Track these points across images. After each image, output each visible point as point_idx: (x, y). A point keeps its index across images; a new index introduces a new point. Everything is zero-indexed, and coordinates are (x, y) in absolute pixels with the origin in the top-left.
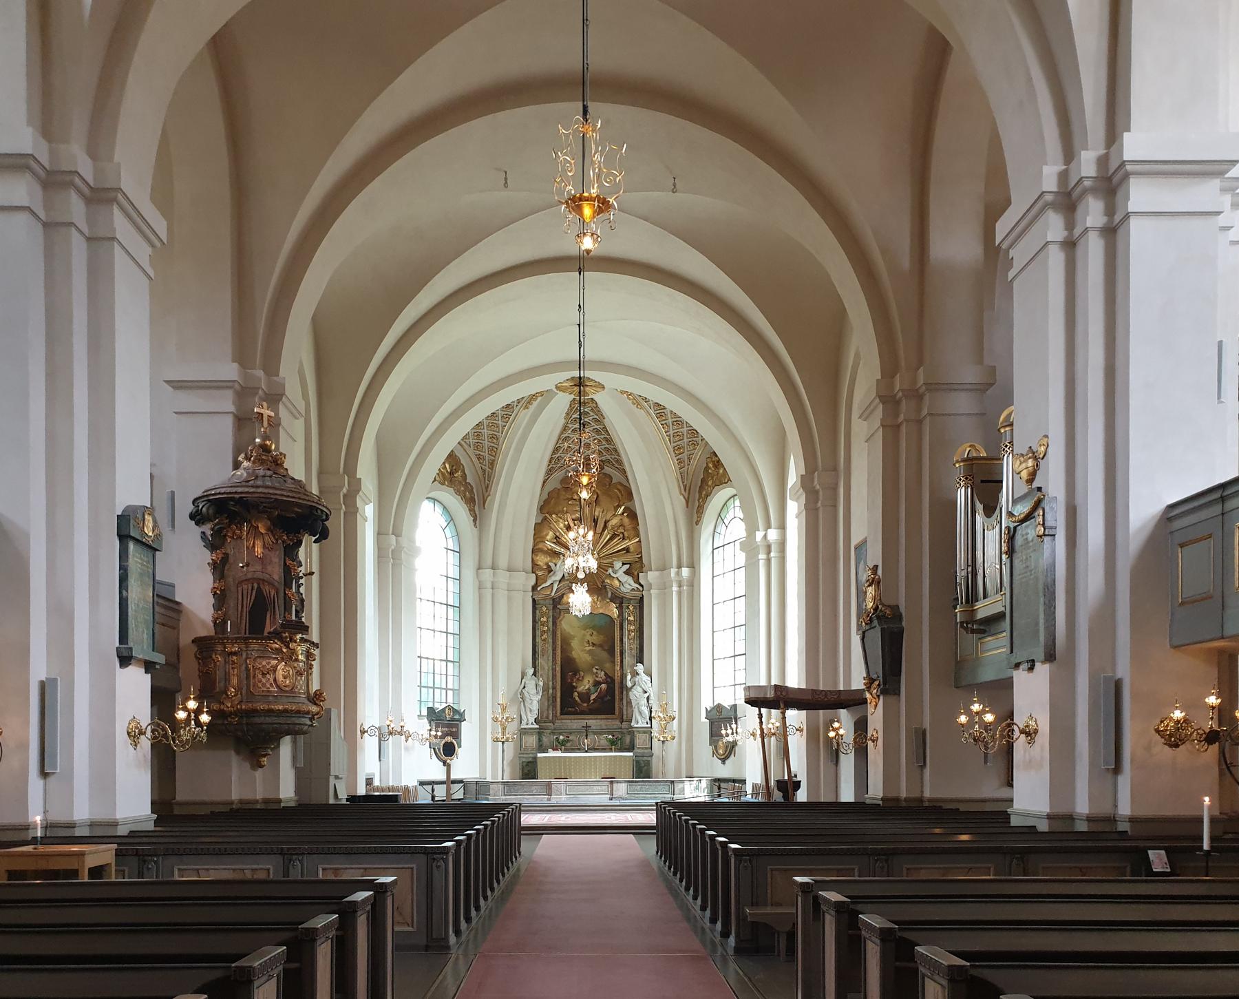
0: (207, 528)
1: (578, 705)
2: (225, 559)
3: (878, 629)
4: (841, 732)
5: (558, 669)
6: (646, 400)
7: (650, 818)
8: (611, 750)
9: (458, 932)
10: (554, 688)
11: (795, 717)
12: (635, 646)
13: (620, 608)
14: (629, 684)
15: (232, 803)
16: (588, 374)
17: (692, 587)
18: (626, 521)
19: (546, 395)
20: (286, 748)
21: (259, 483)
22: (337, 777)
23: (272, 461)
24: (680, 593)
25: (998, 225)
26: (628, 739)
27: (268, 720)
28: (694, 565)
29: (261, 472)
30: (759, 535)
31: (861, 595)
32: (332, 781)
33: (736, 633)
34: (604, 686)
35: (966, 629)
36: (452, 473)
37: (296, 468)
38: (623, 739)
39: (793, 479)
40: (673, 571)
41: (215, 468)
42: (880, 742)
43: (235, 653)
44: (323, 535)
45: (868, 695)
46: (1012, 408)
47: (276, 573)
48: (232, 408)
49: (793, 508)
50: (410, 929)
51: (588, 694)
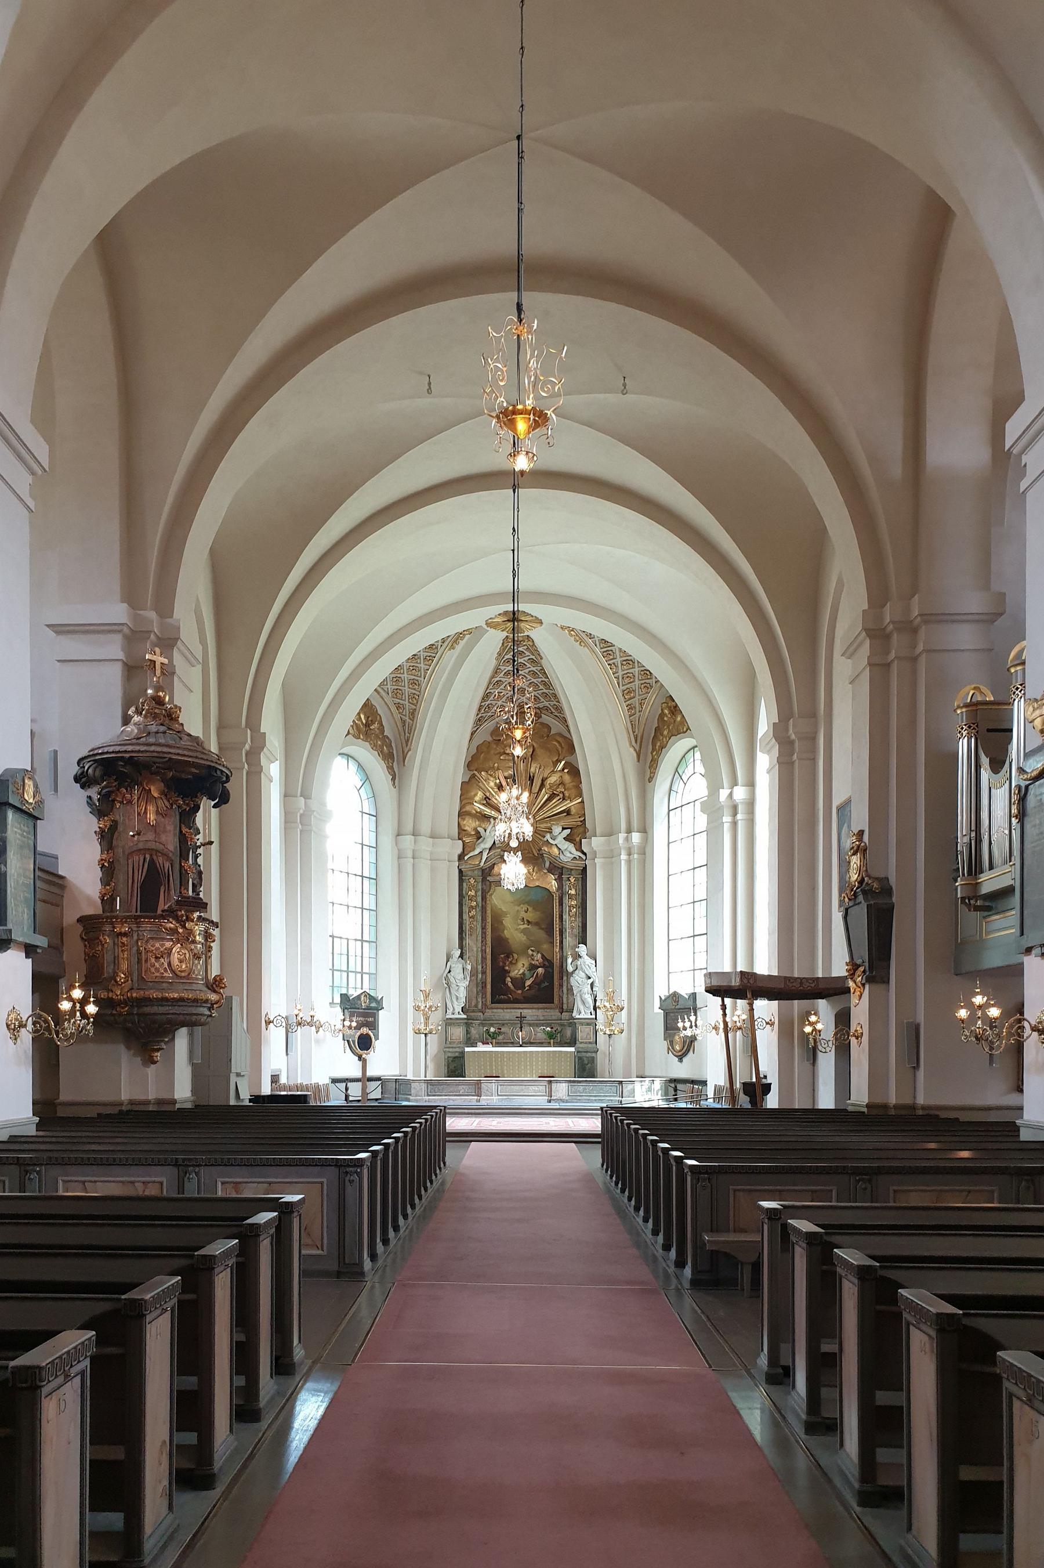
0: (94, 792)
1: (511, 992)
2: (114, 827)
3: (864, 905)
4: (819, 1026)
5: (489, 950)
6: (590, 636)
7: (593, 1125)
8: (549, 1045)
9: (373, 1257)
10: (484, 973)
11: (765, 1008)
12: (578, 923)
13: (559, 880)
14: (570, 969)
15: (121, 1104)
16: (523, 607)
17: (645, 851)
18: (567, 778)
19: (473, 634)
20: (181, 1041)
21: (152, 740)
22: (238, 1075)
23: (166, 716)
24: (629, 862)
25: (1008, 426)
26: (568, 1032)
27: (162, 1010)
28: (645, 830)
29: (153, 728)
30: (724, 794)
31: (844, 865)
32: (233, 1079)
33: (698, 911)
34: (540, 970)
35: (969, 906)
36: (367, 725)
37: (192, 722)
38: (563, 1033)
39: (763, 727)
40: (622, 836)
41: (103, 725)
42: (865, 1039)
43: (125, 934)
44: (223, 799)
45: (851, 984)
46: (1024, 643)
47: (170, 842)
48: (121, 655)
49: (764, 762)
50: (320, 1252)
51: (522, 979)
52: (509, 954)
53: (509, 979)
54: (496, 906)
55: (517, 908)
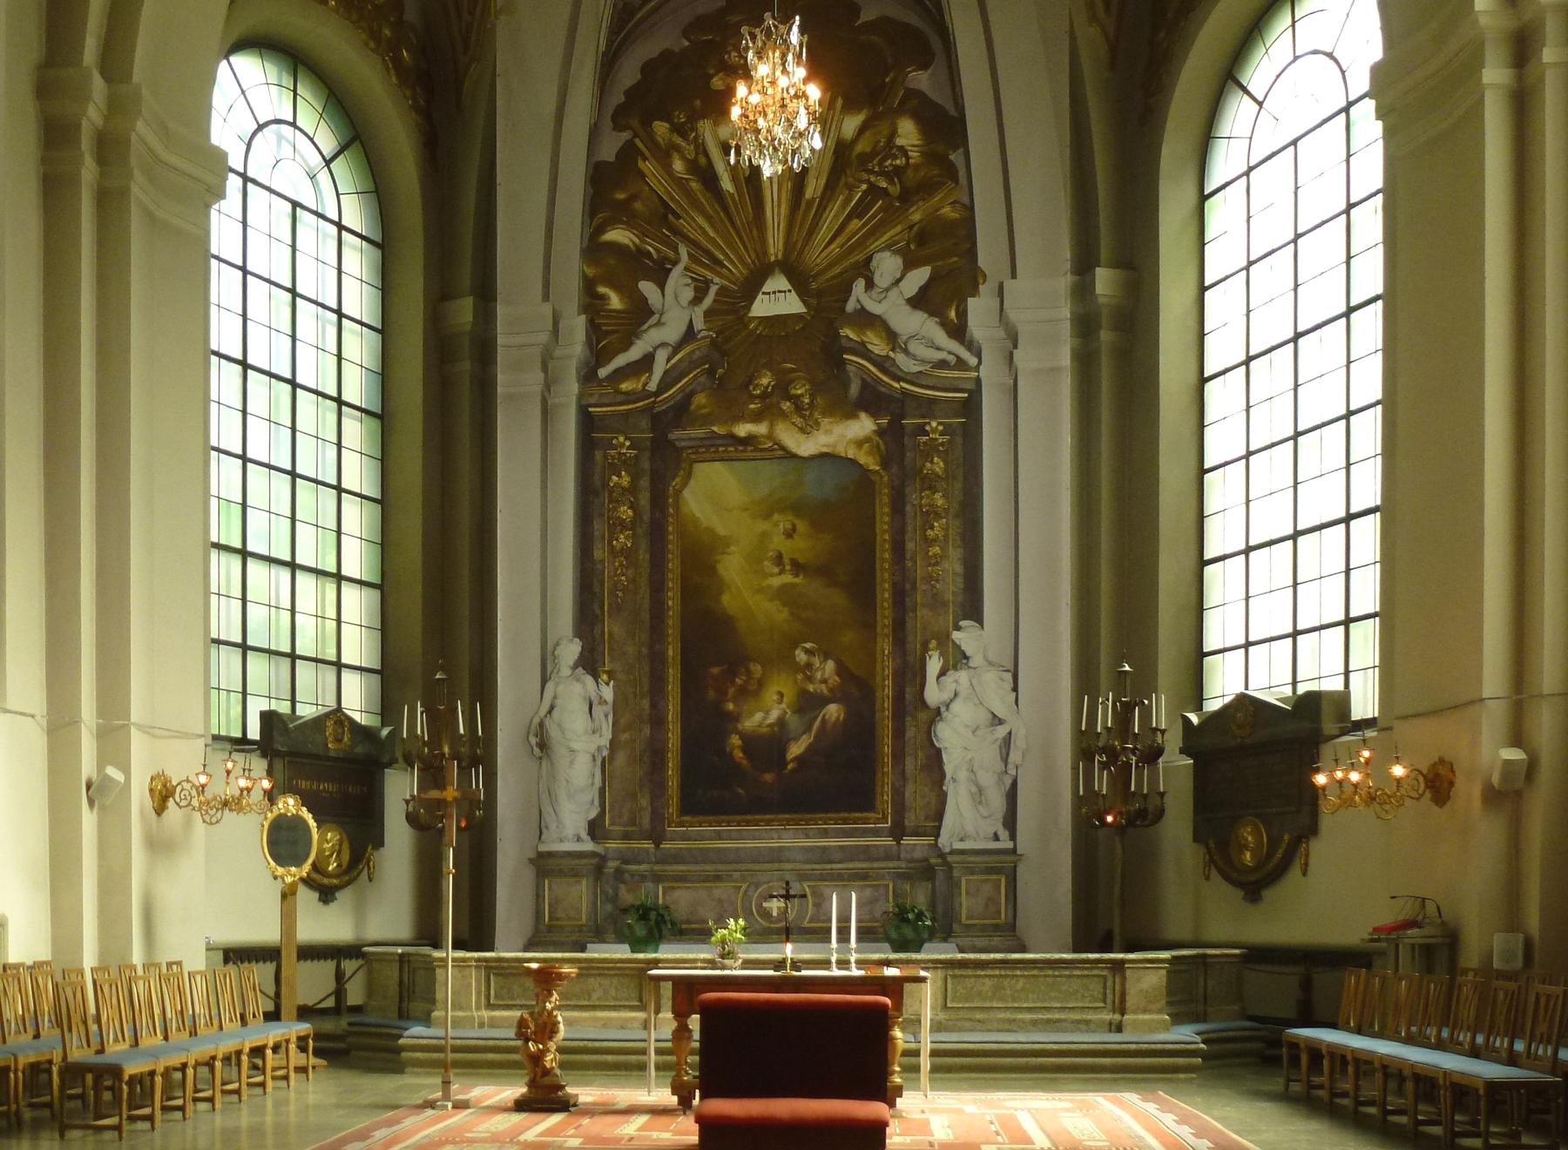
5: (672, 651)
34: (833, 711)
51: (776, 740)
52: (736, 662)
53: (735, 740)
54: (696, 521)
55: (764, 526)
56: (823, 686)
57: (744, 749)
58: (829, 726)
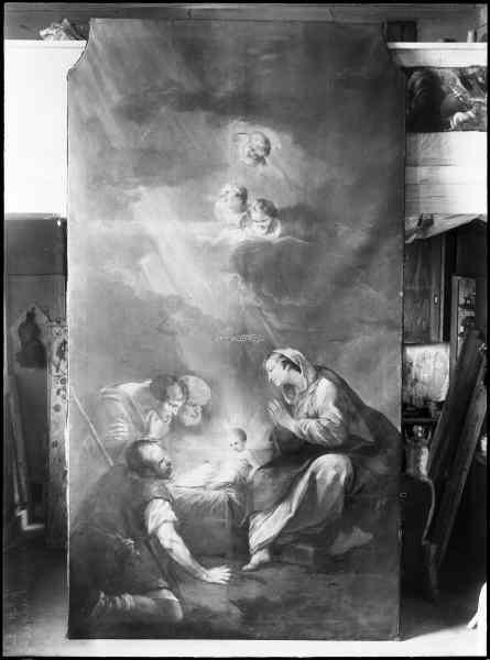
34: (330, 467)
56: (312, 423)
57: (181, 528)
58: (321, 490)
